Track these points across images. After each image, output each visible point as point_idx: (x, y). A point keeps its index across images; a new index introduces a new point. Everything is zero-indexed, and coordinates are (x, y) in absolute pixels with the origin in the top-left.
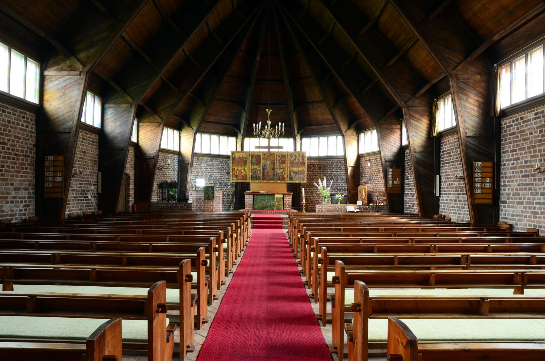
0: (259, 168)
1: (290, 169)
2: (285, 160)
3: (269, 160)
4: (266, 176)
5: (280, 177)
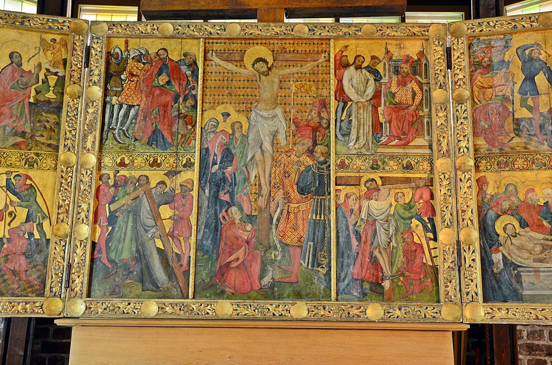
0: (172, 173)
1: (481, 183)
2: (428, 100)
3: (275, 104)
4: (240, 253)
5: (384, 261)
